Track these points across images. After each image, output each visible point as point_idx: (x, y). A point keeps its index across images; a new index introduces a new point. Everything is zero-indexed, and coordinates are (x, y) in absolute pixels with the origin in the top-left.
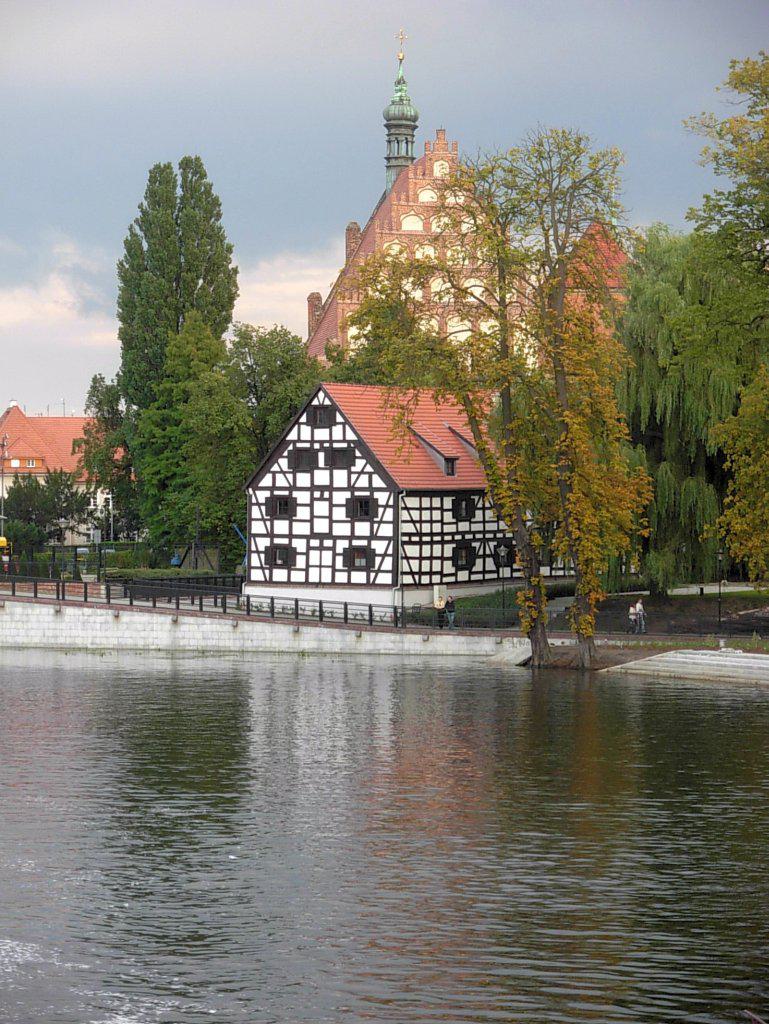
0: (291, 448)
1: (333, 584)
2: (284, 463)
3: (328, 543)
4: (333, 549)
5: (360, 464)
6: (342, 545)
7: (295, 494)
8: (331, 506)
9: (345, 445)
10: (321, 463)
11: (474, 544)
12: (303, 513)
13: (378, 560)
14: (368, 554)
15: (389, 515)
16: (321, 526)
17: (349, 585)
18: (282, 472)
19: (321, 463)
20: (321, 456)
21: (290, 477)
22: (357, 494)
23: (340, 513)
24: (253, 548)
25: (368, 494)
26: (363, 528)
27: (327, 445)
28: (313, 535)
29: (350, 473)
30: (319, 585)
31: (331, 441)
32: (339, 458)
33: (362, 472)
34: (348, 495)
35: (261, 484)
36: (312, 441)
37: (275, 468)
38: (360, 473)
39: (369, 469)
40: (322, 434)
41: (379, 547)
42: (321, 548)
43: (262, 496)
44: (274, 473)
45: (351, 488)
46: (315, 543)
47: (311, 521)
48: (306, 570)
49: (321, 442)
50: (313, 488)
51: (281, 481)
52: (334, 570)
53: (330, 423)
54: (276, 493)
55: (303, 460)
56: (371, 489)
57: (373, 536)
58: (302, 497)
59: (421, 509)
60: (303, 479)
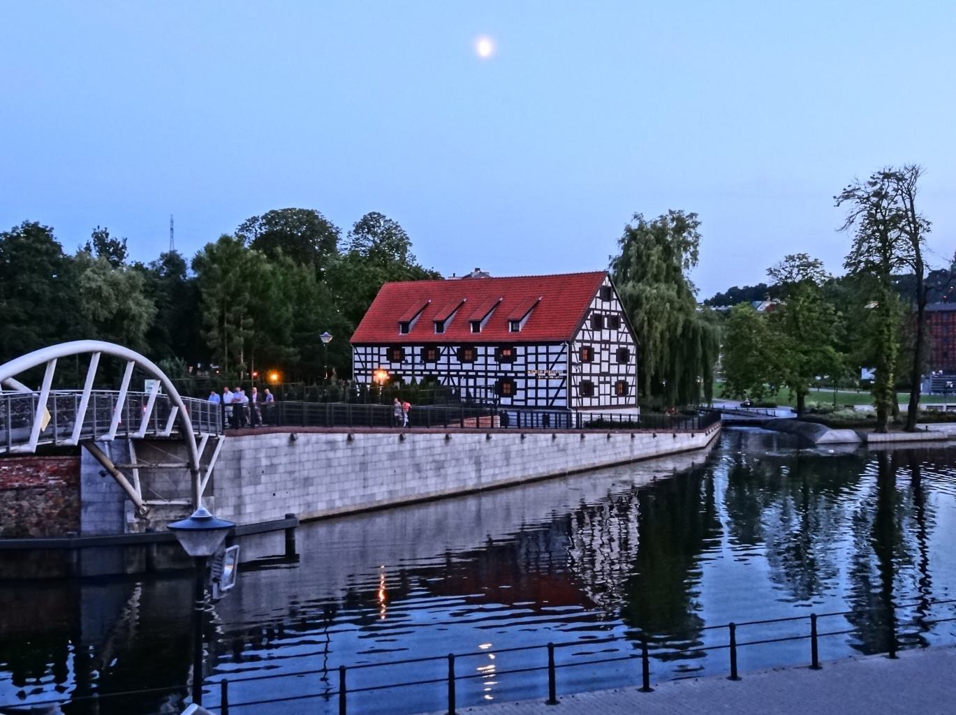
0: (591, 313)
1: (611, 407)
2: (588, 323)
3: (608, 379)
4: (610, 382)
5: (623, 326)
6: (614, 379)
7: (594, 346)
8: (610, 354)
9: (616, 314)
10: (606, 326)
11: (439, 378)
12: (597, 358)
13: (630, 388)
14: (625, 384)
15: (633, 360)
16: (605, 368)
17: (618, 406)
18: (587, 330)
19: (606, 326)
20: (606, 319)
21: (591, 333)
22: (621, 346)
23: (613, 359)
24: (573, 384)
25: (625, 346)
26: (623, 368)
27: (608, 313)
28: (602, 374)
29: (618, 332)
30: (605, 407)
31: (610, 311)
32: (614, 324)
33: (623, 333)
34: (616, 347)
35: (577, 338)
36: (602, 310)
37: (584, 327)
38: (623, 333)
39: (626, 330)
40: (606, 306)
41: (630, 380)
42: (605, 382)
43: (577, 346)
44: (584, 330)
45: (618, 343)
46: (602, 379)
47: (600, 364)
48: (598, 398)
49: (606, 311)
50: (602, 342)
51: (587, 337)
52: (611, 397)
53: (609, 299)
54: (584, 344)
55: (598, 324)
56: (626, 343)
57: (627, 374)
58: (596, 347)
59: (366, 354)
60: (597, 336)
